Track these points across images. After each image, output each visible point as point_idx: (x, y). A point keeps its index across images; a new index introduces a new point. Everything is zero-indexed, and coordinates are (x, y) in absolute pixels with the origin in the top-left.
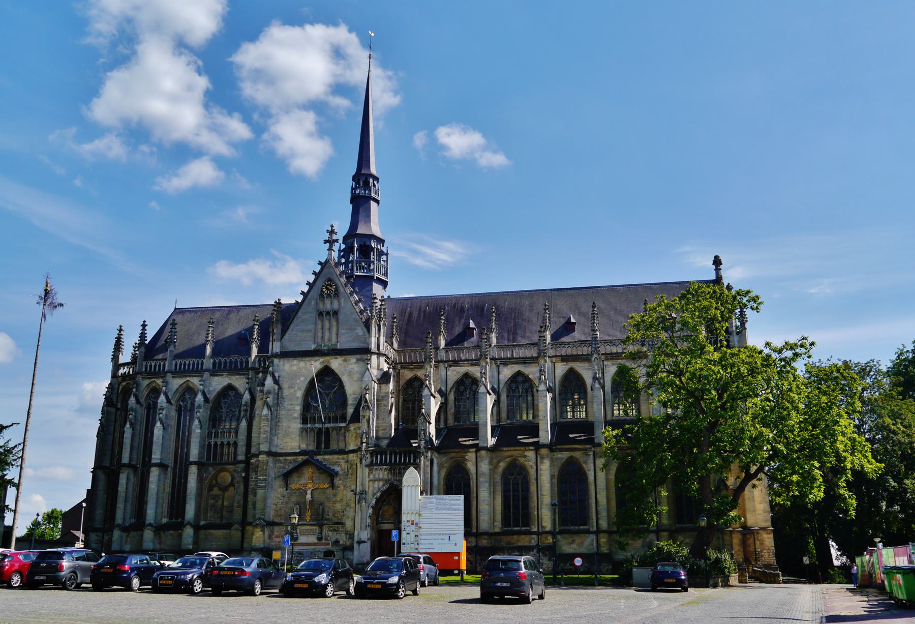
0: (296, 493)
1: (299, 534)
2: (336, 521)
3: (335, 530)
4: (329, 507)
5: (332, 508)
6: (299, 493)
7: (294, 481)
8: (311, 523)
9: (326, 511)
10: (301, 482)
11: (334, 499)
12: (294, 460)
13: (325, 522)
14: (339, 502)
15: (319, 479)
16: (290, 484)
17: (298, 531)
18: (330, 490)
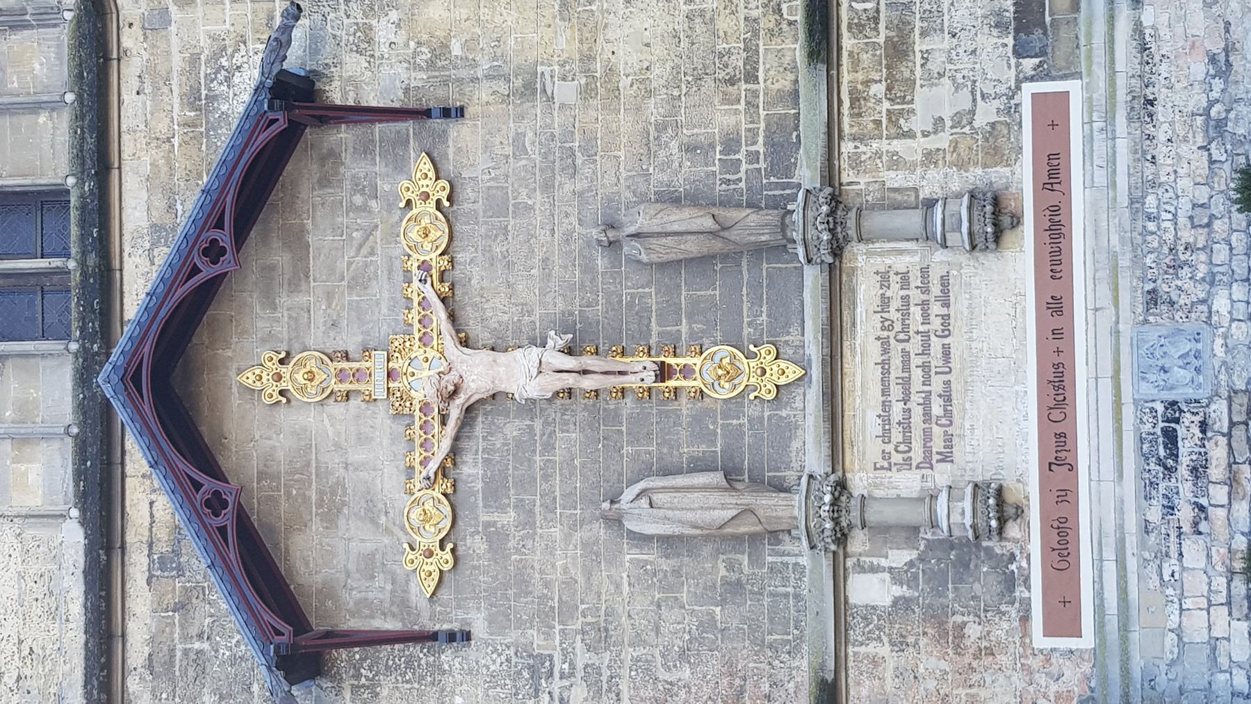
0: (496, 538)
1: (942, 475)
2: (795, 48)
3: (898, 50)
4: (649, 142)
5: (654, 110)
6: (494, 493)
7: (370, 565)
8: (814, 350)
9: (684, 173)
10: (389, 483)
11: (566, 92)
12: (166, 564)
13: (807, 174)
14: (590, 31)
15: (359, 282)
16: (404, 605)
17: (908, 483)
18: (460, 134)
